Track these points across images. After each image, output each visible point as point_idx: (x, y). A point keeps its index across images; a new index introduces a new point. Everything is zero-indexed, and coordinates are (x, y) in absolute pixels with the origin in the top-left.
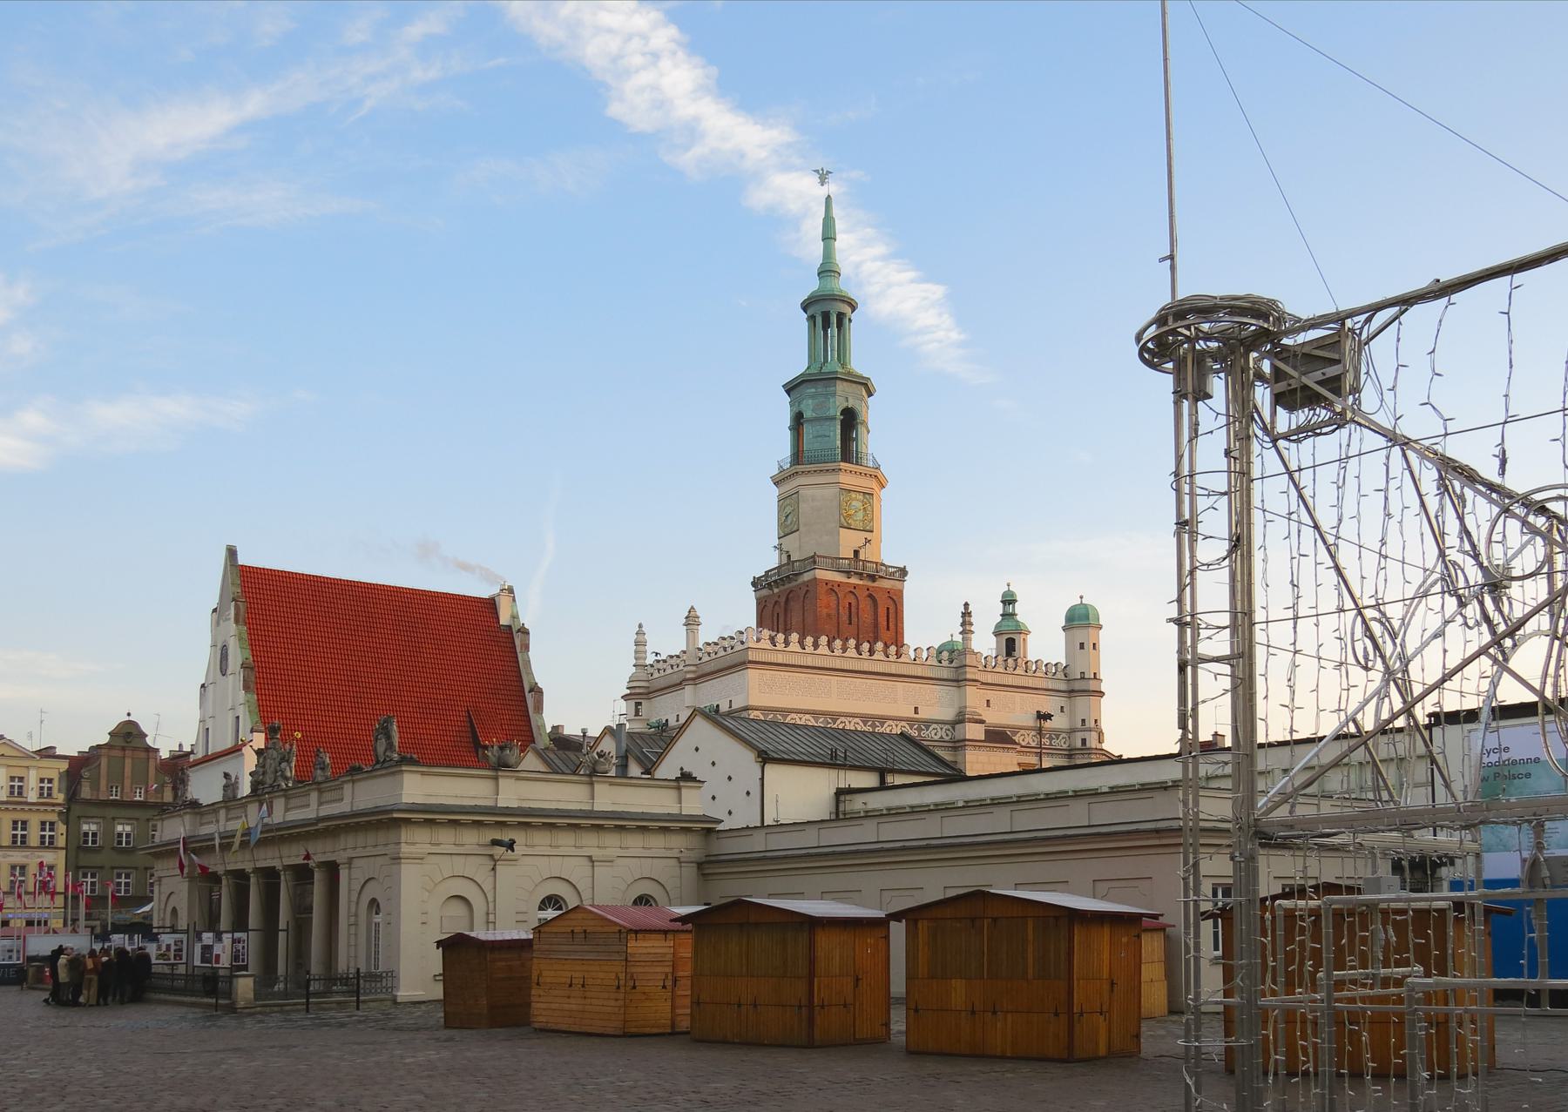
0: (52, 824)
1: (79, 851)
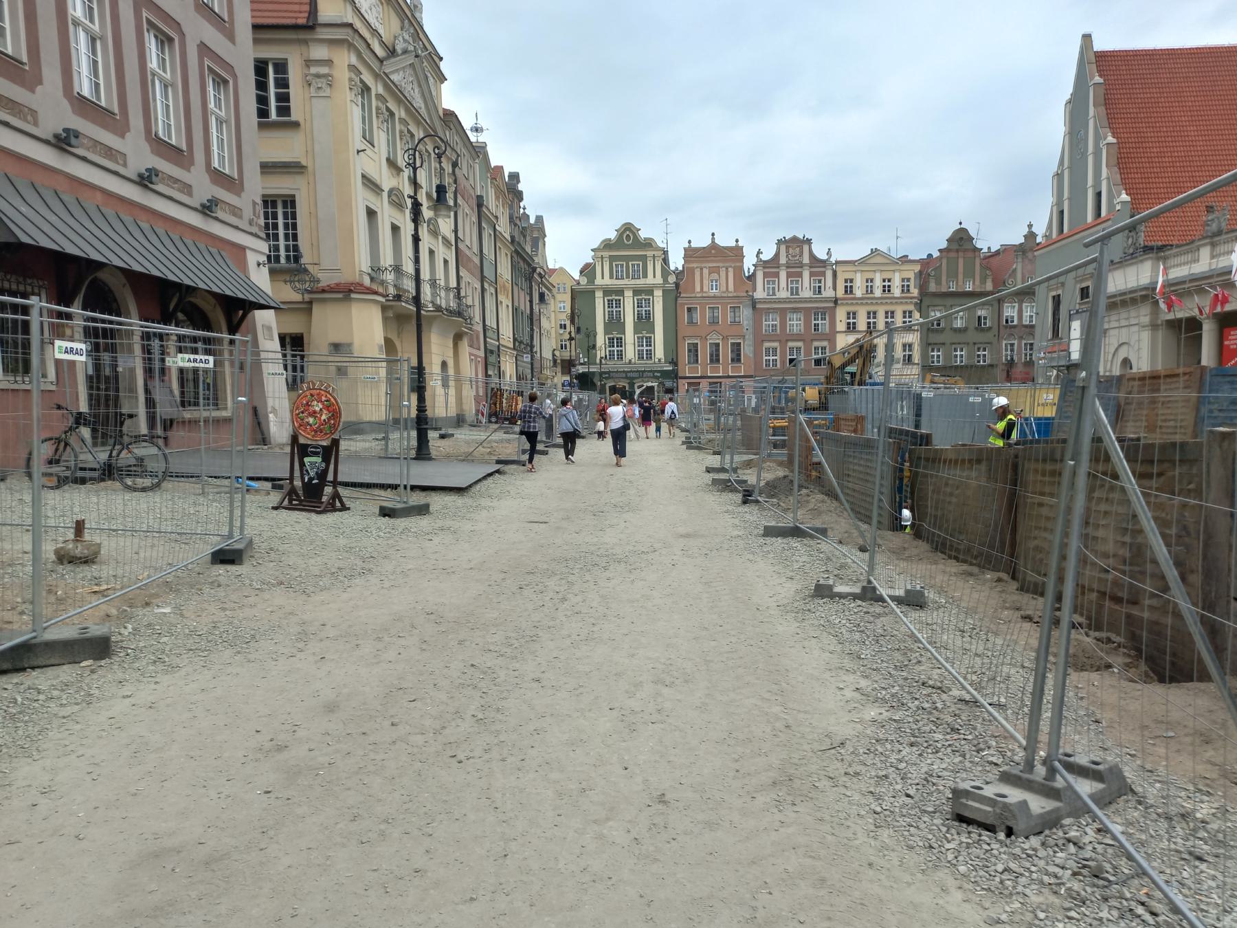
0: (910, 312)
1: (931, 333)
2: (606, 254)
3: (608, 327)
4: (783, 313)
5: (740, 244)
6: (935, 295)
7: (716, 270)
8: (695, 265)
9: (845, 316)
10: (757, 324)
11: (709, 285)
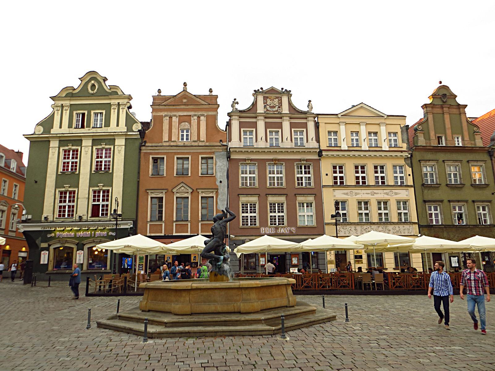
0: (401, 167)
2: (67, 103)
3: (61, 179)
4: (262, 163)
5: (213, 93)
6: (425, 149)
7: (188, 119)
8: (163, 114)
9: (330, 170)
10: (231, 176)
11: (174, 133)
